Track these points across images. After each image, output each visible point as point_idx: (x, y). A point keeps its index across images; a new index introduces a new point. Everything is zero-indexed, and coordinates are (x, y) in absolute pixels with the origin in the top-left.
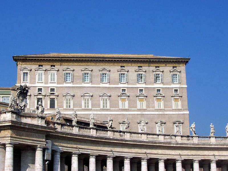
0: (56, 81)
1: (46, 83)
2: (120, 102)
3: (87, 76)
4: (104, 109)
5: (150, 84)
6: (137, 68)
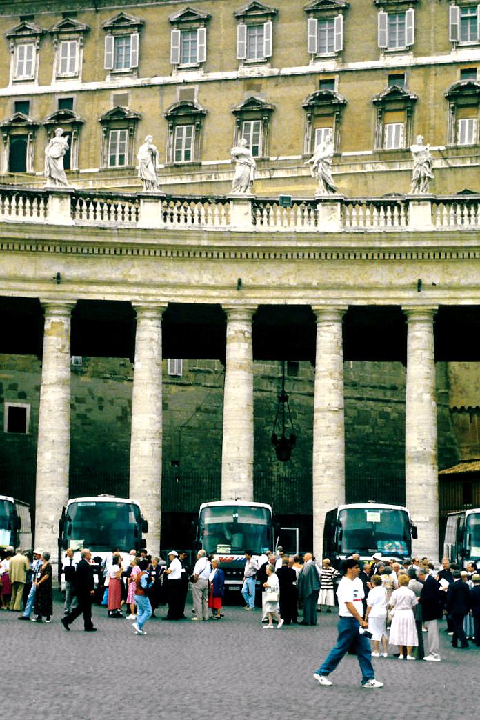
0: (78, 67)
3: (192, 42)
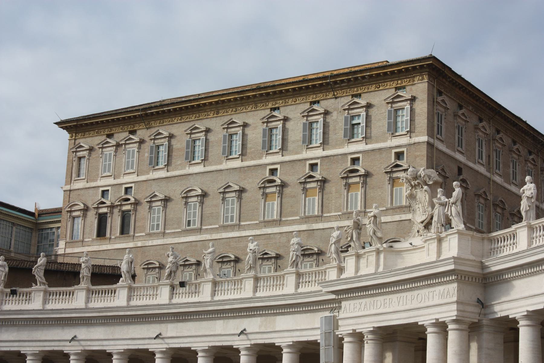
4: (228, 226)
5: (334, 147)
6: (307, 106)
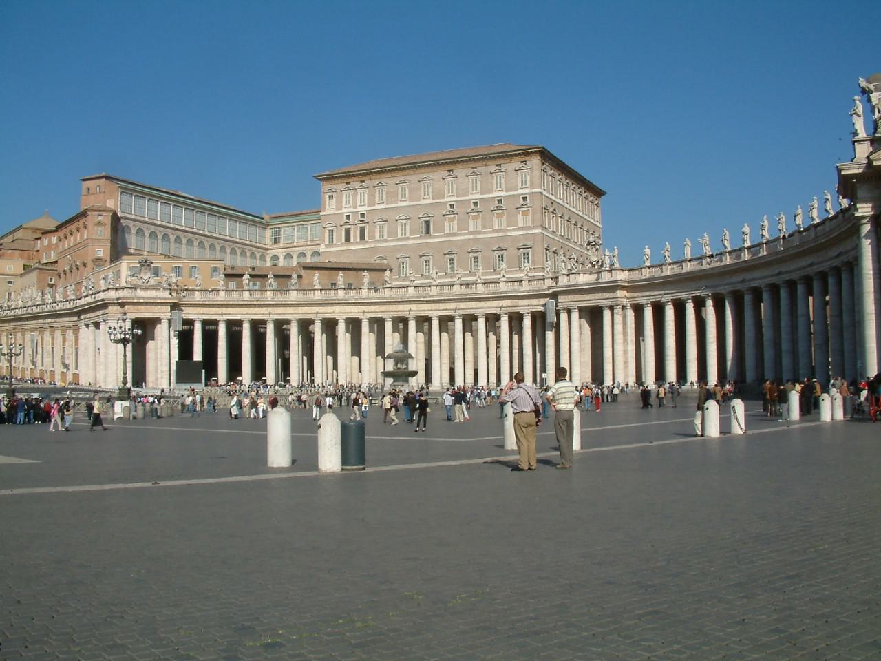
0: (366, 201)
1: (355, 207)
2: (447, 224)
